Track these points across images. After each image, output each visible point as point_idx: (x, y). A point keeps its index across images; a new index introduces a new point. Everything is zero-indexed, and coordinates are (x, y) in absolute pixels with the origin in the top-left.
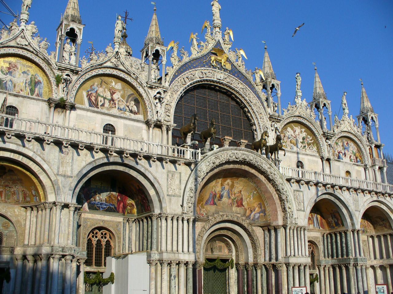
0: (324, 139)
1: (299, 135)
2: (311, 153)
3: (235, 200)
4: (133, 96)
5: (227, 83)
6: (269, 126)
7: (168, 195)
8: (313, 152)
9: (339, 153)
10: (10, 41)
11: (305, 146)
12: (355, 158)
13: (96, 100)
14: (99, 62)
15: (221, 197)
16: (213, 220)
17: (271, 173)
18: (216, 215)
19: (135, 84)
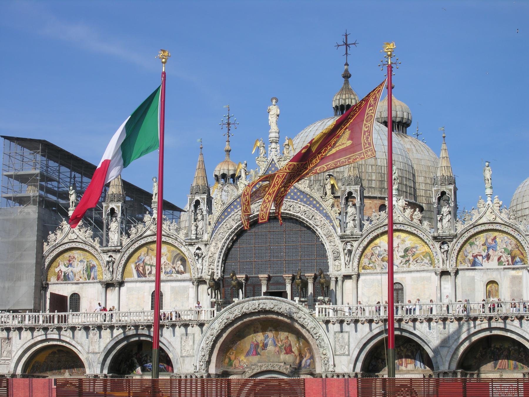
0: (437, 245)
1: (398, 247)
2: (418, 268)
3: (283, 348)
4: (180, 255)
5: (285, 210)
6: (341, 250)
7: (181, 357)
8: (423, 265)
9: (475, 257)
10: (64, 238)
11: (409, 260)
12: (510, 259)
13: (144, 269)
14: (139, 234)
15: (265, 346)
16: (250, 372)
17: (300, 318)
18: (253, 367)
19: (176, 245)
